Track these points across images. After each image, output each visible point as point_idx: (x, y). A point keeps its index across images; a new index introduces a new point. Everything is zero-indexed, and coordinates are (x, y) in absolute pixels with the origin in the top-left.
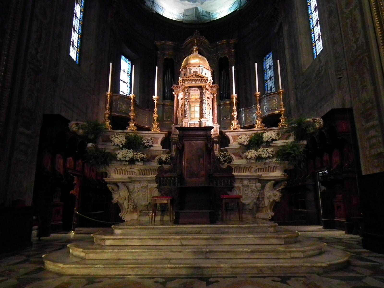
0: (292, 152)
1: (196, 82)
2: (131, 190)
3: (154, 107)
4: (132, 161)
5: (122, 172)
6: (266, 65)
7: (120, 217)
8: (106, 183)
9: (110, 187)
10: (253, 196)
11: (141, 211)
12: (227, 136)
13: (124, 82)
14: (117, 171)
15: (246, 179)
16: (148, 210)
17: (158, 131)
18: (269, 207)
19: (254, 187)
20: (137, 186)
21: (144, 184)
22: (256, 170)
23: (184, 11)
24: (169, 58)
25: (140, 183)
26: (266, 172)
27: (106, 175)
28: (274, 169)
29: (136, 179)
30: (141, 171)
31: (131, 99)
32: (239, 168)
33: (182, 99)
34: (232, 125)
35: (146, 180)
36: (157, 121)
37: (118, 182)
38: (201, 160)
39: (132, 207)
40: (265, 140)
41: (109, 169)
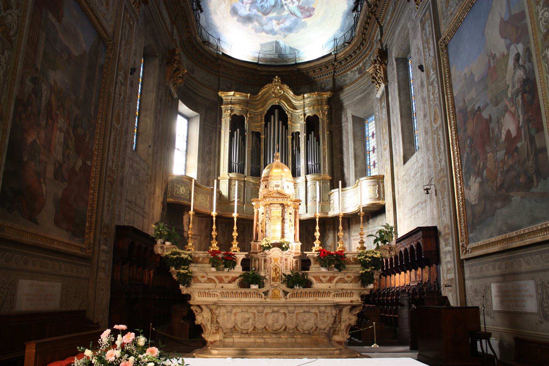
1: (277, 200)
2: (217, 315)
3: (234, 225)
5: (205, 295)
6: (368, 130)
7: (203, 337)
8: (191, 305)
10: (329, 321)
11: (226, 333)
13: (178, 149)
14: (201, 294)
15: (322, 306)
16: (232, 333)
17: (238, 251)
18: (344, 331)
20: (223, 310)
22: (334, 295)
23: (260, 46)
25: (225, 308)
26: (343, 297)
28: (351, 294)
29: (222, 304)
30: (223, 294)
31: (213, 217)
33: (263, 214)
34: (314, 246)
35: (231, 306)
36: (237, 240)
37: (202, 305)
39: (215, 328)
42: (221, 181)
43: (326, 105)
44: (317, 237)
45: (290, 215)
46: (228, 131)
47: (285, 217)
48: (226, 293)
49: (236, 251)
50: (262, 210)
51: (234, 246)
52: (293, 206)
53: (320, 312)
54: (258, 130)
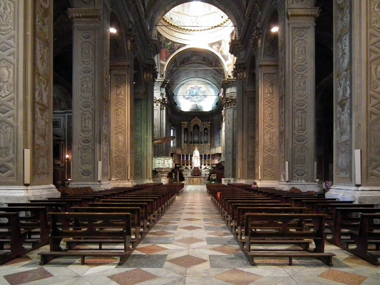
32: (203, 172)
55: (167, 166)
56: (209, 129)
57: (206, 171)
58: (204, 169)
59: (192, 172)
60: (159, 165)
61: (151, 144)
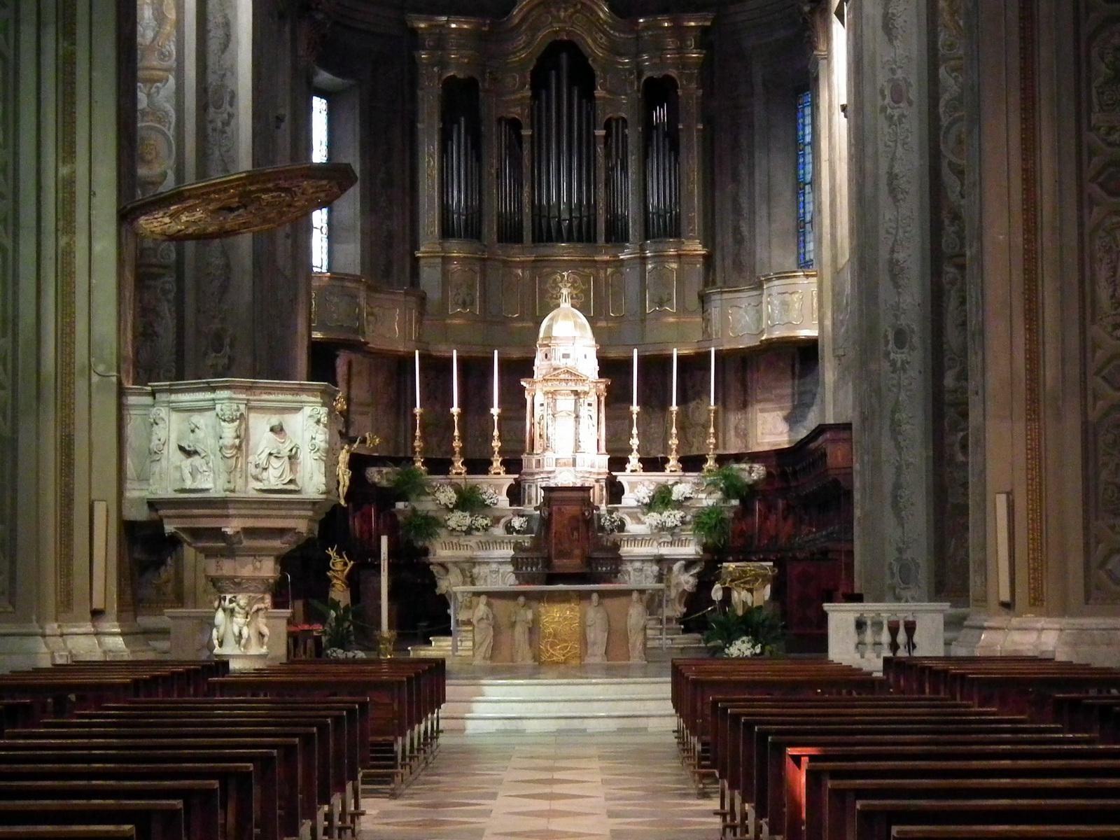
0: (709, 521)
4: (469, 531)
9: (434, 569)
12: (620, 482)
17: (502, 472)
18: (677, 601)
19: (649, 572)
21: (494, 566)
24: (461, 76)
27: (426, 551)
32: (635, 539)
33: (542, 405)
37: (448, 562)
38: (576, 534)
40: (674, 497)
41: (434, 542)
42: (422, 262)
43: (695, 48)
44: (635, 447)
45: (590, 408)
46: (437, 125)
47: (581, 414)
48: (485, 543)
49: (499, 474)
50: (539, 398)
51: (495, 464)
52: (594, 390)
53: (635, 570)
54: (513, 113)
55: (274, 477)
56: (690, 91)
57: (662, 528)
58: (650, 507)
59: (526, 540)
60: (187, 463)
61: (106, 246)
